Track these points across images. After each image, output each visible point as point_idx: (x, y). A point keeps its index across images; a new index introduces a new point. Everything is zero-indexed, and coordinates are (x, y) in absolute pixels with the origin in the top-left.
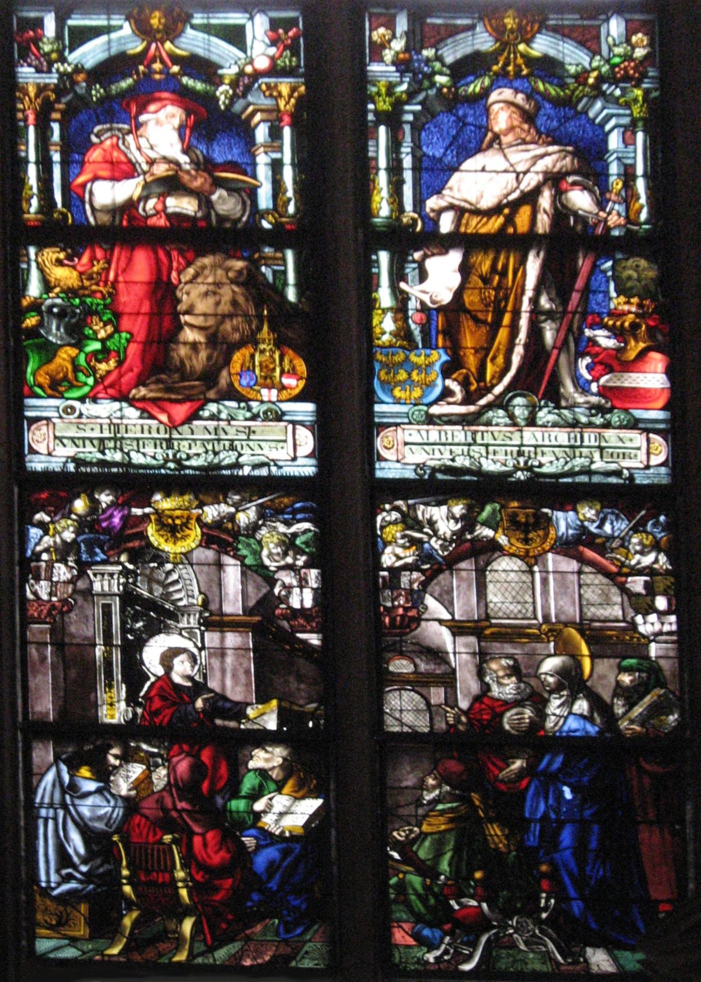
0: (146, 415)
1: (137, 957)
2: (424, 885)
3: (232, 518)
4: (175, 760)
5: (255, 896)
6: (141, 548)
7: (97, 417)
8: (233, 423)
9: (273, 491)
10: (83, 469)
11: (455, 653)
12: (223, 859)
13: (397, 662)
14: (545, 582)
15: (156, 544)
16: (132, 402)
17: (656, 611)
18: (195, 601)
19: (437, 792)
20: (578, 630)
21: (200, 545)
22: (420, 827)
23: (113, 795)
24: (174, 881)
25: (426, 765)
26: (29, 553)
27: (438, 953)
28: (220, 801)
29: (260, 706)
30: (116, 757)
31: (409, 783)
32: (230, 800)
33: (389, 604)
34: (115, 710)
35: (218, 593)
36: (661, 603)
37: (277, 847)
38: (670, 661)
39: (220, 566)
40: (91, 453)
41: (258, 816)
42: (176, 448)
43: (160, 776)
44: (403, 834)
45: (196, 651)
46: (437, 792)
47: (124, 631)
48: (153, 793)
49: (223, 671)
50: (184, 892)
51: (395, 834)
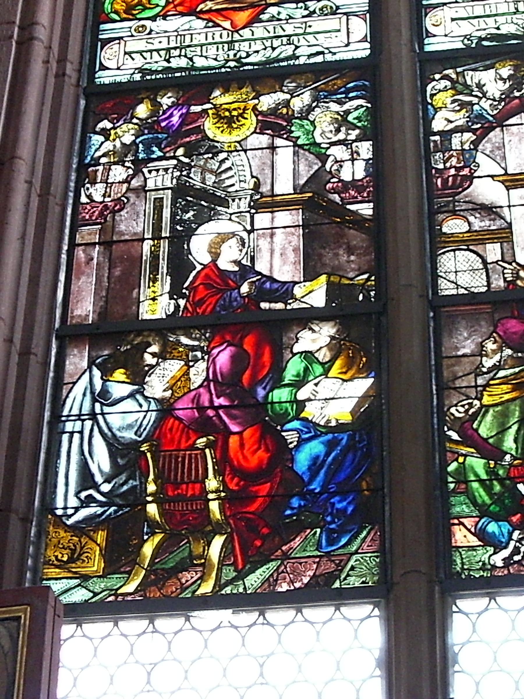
0: (210, 24)
1: (154, 593)
2: (487, 467)
3: (287, 104)
4: (215, 351)
5: (295, 502)
6: (198, 141)
7: (166, 32)
8: (290, 21)
9: (327, 77)
10: (148, 77)
12: (261, 460)
13: (451, 223)
15: (211, 136)
16: (198, 14)
18: (246, 186)
19: (497, 357)
21: (255, 132)
22: (480, 399)
23: (146, 398)
24: (204, 492)
25: (485, 328)
26: (89, 158)
27: (505, 553)
28: (261, 392)
29: (307, 284)
30: (154, 355)
31: (467, 351)
32: (271, 390)
33: (441, 166)
34: (156, 303)
35: (270, 176)
37: (321, 439)
39: (272, 148)
40: (158, 63)
41: (301, 405)
42: (237, 48)
43: (198, 373)
44: (462, 409)
45: (245, 235)
47: (174, 221)
48: (190, 391)
50: (214, 506)
51: (453, 410)
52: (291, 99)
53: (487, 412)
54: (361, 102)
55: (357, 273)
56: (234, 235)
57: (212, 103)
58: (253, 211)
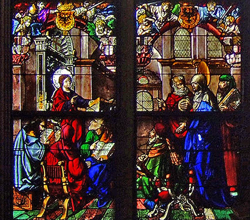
11: (162, 74)
14: (195, 40)
17: (234, 53)
20: (206, 62)
29: (93, 101)
36: (236, 49)
38: (238, 76)
46: (154, 139)
49: (81, 85)
52: (87, 11)
53: (150, 160)
54: (112, 16)
55: (110, 98)
56: (67, 76)
57: (58, 10)
58: (74, 65)
